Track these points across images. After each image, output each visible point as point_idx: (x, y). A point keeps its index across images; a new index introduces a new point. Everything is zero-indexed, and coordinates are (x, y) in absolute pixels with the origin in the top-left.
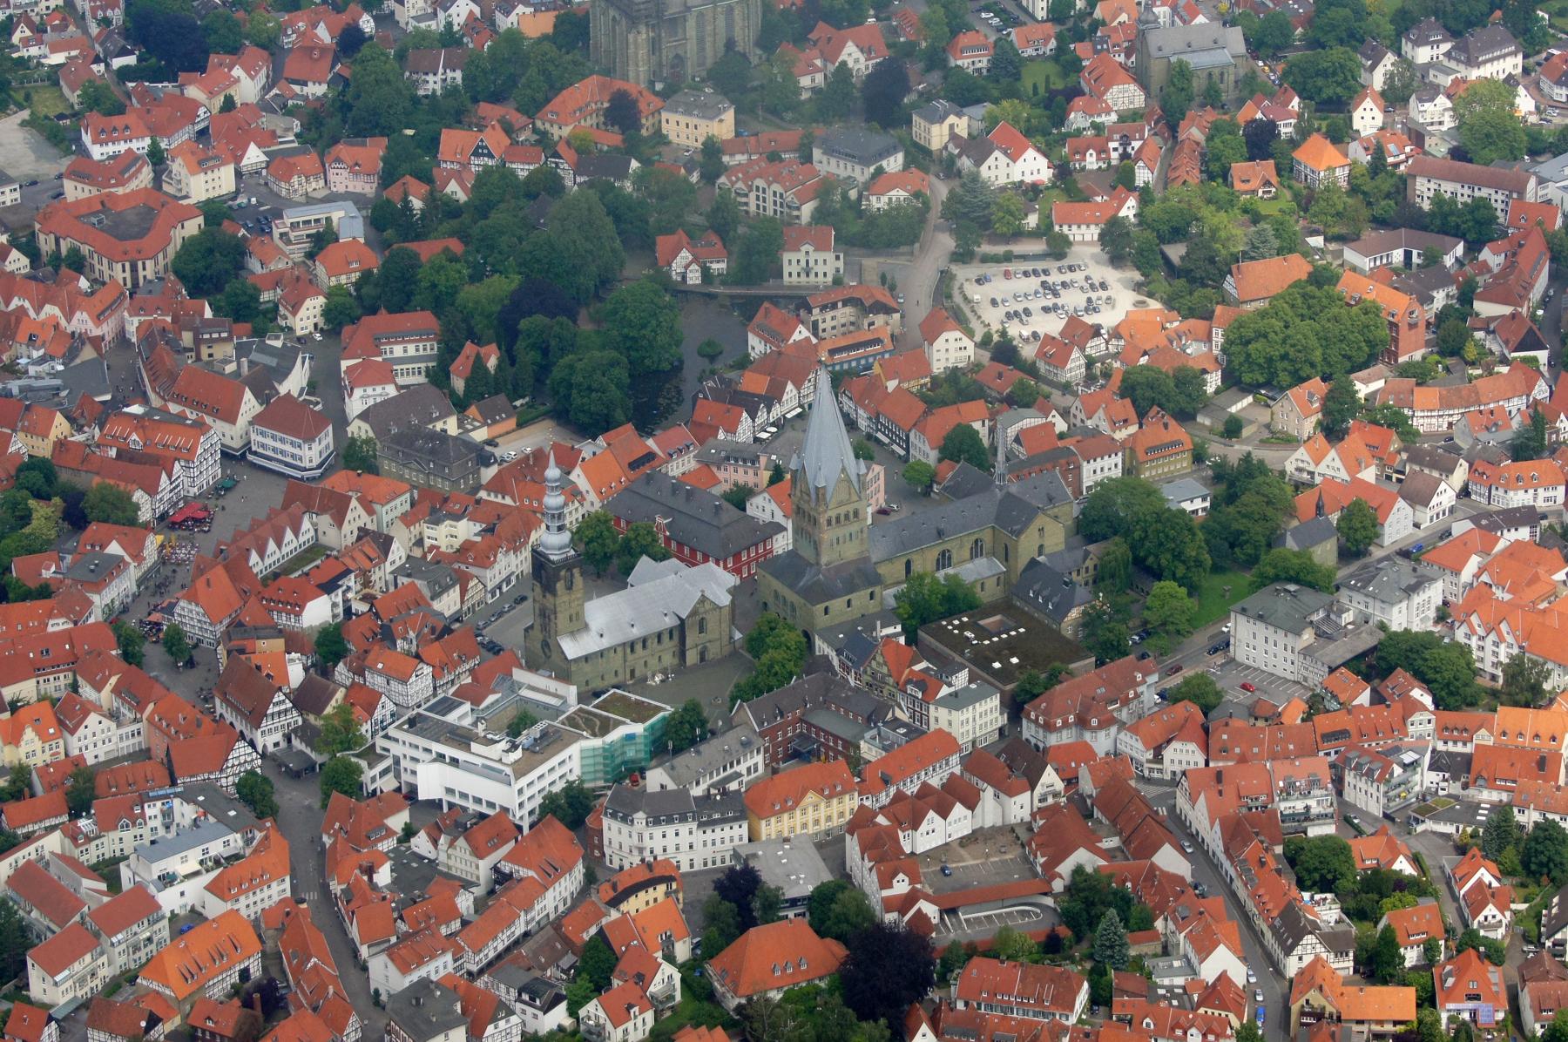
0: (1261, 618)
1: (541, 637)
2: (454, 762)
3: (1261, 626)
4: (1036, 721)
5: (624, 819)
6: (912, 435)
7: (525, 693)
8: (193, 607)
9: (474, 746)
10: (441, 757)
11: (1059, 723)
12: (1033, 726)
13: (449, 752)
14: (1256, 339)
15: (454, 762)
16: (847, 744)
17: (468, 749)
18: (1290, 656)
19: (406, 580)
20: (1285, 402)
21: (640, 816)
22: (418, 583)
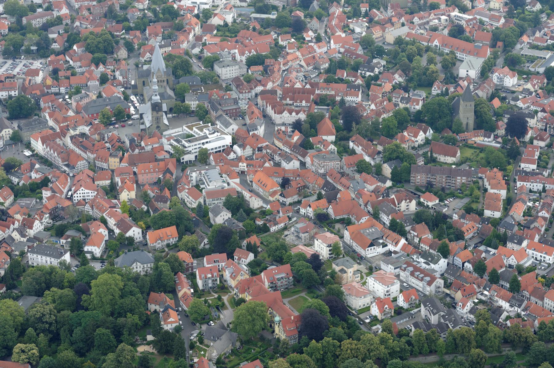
0: (228, 66)
1: (156, 126)
2: (207, 142)
3: (228, 68)
4: (245, 92)
5: (256, 129)
6: (89, 83)
7: (173, 135)
8: (82, 162)
9: (209, 136)
10: (203, 144)
11: (244, 92)
12: (244, 95)
13: (204, 141)
14: (98, 44)
15: (207, 142)
16: (236, 109)
17: (208, 138)
18: (236, 71)
19: (110, 134)
20: (122, 51)
21: (259, 127)
22: (114, 132)
